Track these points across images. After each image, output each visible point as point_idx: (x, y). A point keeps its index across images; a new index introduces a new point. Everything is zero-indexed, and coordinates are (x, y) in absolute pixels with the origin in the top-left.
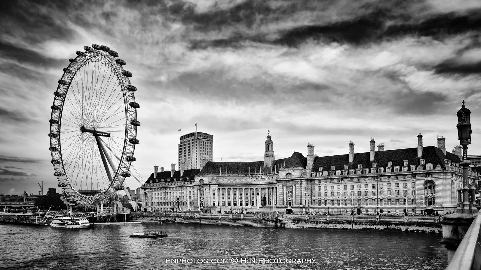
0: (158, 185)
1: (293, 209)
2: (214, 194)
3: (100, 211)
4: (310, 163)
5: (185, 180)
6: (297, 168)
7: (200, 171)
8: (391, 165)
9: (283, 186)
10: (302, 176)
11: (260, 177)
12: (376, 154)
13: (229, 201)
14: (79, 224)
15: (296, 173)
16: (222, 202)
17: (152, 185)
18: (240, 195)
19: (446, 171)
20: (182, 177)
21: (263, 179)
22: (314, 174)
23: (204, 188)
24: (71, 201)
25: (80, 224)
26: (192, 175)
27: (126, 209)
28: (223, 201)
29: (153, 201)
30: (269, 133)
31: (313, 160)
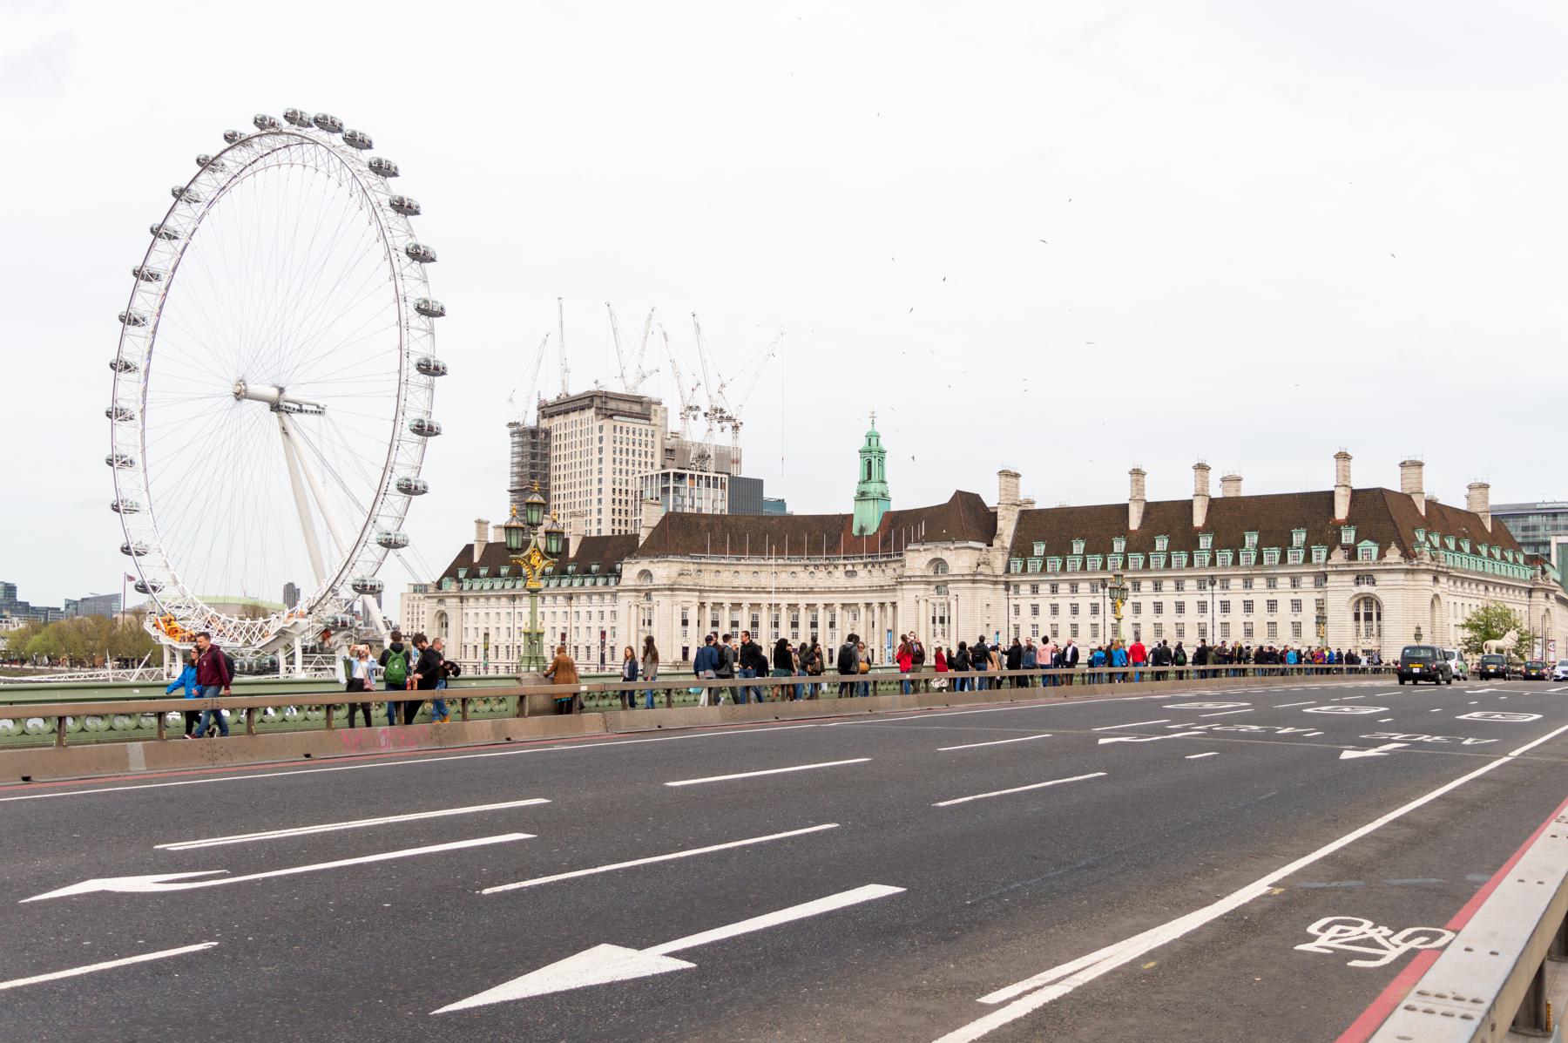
0: (487, 586)
2: (685, 623)
4: (1007, 527)
6: (965, 545)
7: (641, 543)
8: (1256, 542)
10: (980, 569)
11: (841, 568)
12: (1213, 504)
15: (960, 559)
17: (466, 586)
19: (1415, 567)
20: (575, 560)
21: (851, 574)
22: (1017, 565)
23: (655, 599)
26: (608, 555)
31: (1016, 517)
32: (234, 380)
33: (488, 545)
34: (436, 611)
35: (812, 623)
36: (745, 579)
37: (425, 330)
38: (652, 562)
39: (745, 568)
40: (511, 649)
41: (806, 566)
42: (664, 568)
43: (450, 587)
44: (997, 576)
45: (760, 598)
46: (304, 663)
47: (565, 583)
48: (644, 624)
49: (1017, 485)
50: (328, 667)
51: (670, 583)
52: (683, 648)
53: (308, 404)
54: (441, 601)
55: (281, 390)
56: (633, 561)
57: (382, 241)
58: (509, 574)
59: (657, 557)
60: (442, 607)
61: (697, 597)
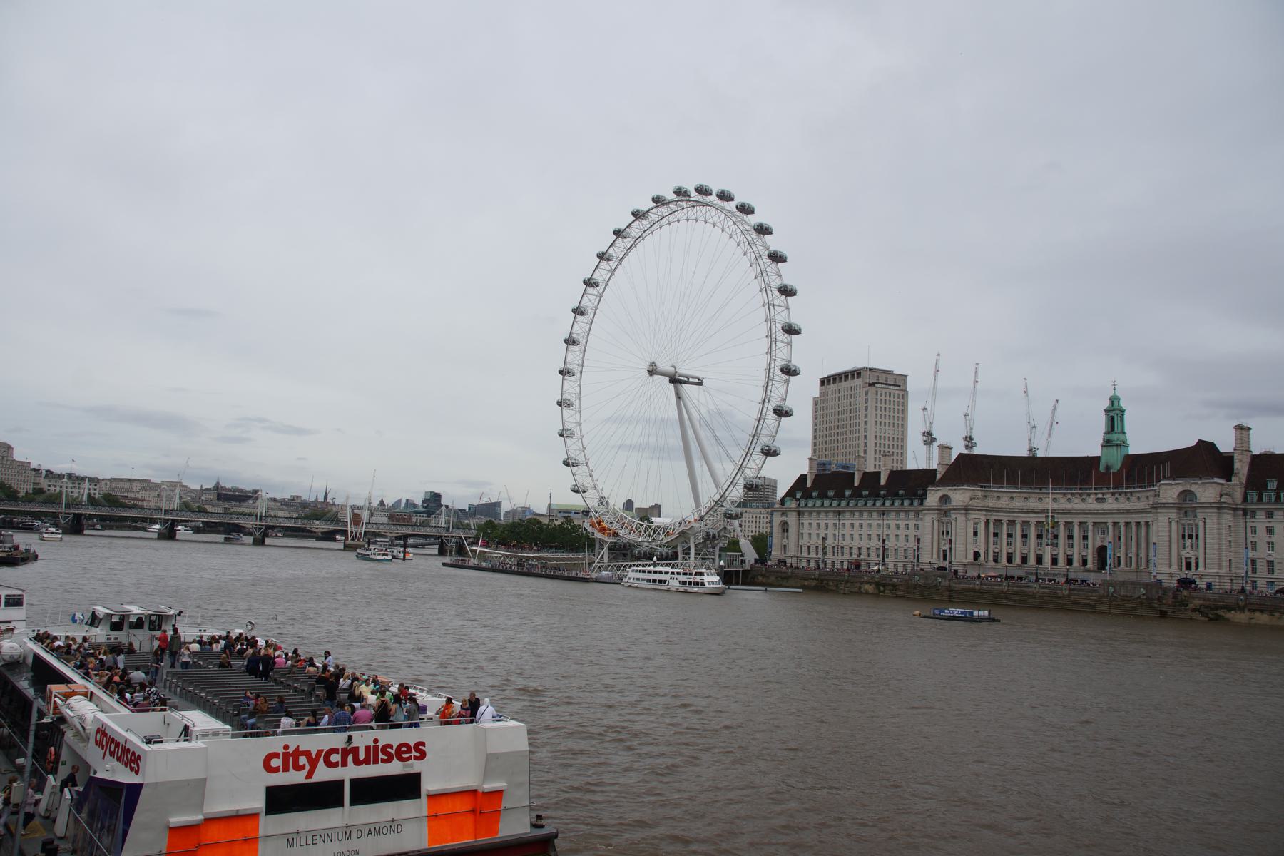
0: (818, 504)
1: (1196, 580)
2: (975, 534)
3: (686, 560)
4: (1241, 467)
5: (893, 495)
6: (1212, 481)
7: (939, 476)
9: (1170, 523)
13: (1010, 551)
14: (703, 584)
15: (1207, 491)
16: (994, 553)
17: (803, 503)
18: (1068, 539)
22: (1253, 496)
23: (953, 516)
24: (610, 534)
25: (706, 584)
27: (740, 558)
28: (996, 550)
29: (805, 541)
30: (1115, 389)
31: (1249, 460)
32: (648, 364)
34: (780, 521)
35: (1068, 536)
36: (1018, 504)
38: (950, 489)
39: (1018, 495)
40: (836, 549)
41: (1065, 494)
43: (791, 504)
44: (1237, 504)
45: (1029, 517)
46: (696, 554)
48: (943, 534)
49: (1249, 436)
52: (975, 552)
53: (693, 378)
59: (955, 486)
60: (784, 518)
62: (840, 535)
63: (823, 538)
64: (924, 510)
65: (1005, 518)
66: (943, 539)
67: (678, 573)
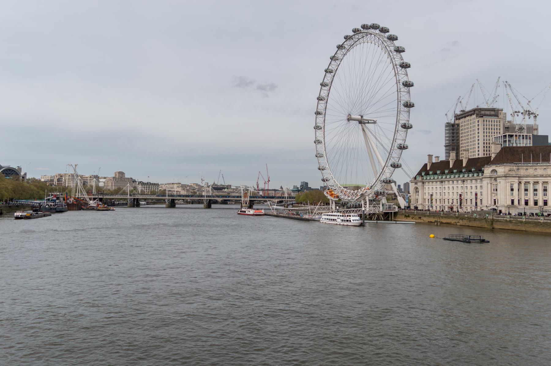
0: (432, 178)
2: (512, 190)
7: (492, 159)
17: (425, 178)
20: (465, 167)
26: (478, 165)
27: (393, 206)
28: (527, 199)
33: (433, 164)
34: (414, 187)
37: (407, 92)
38: (497, 166)
39: (540, 167)
40: (441, 200)
42: (502, 169)
45: (548, 179)
47: (461, 176)
48: (494, 191)
50: (378, 206)
51: (505, 174)
52: (512, 200)
53: (371, 120)
54: (416, 183)
55: (362, 117)
56: (489, 166)
57: (392, 63)
58: (440, 173)
59: (499, 164)
61: (517, 179)
62: (443, 193)
63: (431, 195)
64: (483, 178)
65: (531, 180)
66: (493, 193)
67: (340, 216)
